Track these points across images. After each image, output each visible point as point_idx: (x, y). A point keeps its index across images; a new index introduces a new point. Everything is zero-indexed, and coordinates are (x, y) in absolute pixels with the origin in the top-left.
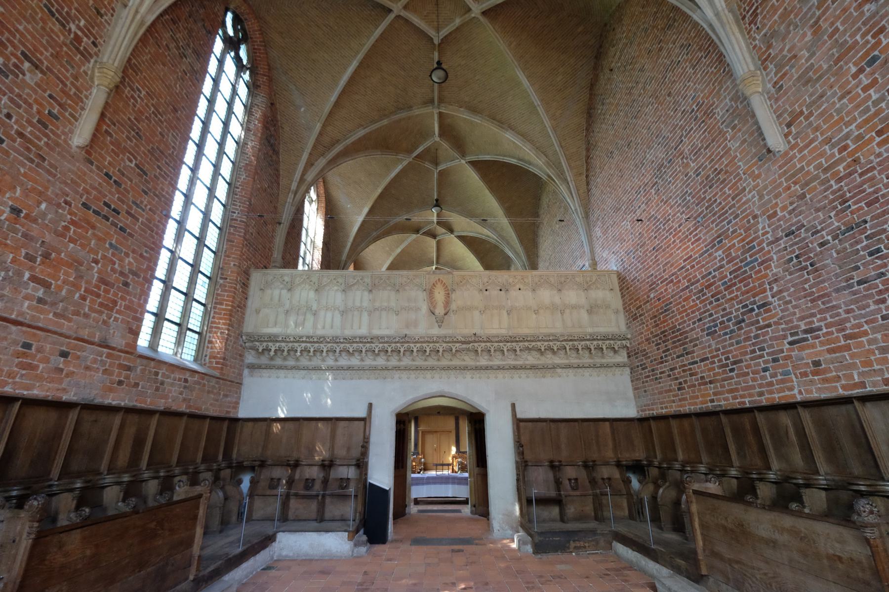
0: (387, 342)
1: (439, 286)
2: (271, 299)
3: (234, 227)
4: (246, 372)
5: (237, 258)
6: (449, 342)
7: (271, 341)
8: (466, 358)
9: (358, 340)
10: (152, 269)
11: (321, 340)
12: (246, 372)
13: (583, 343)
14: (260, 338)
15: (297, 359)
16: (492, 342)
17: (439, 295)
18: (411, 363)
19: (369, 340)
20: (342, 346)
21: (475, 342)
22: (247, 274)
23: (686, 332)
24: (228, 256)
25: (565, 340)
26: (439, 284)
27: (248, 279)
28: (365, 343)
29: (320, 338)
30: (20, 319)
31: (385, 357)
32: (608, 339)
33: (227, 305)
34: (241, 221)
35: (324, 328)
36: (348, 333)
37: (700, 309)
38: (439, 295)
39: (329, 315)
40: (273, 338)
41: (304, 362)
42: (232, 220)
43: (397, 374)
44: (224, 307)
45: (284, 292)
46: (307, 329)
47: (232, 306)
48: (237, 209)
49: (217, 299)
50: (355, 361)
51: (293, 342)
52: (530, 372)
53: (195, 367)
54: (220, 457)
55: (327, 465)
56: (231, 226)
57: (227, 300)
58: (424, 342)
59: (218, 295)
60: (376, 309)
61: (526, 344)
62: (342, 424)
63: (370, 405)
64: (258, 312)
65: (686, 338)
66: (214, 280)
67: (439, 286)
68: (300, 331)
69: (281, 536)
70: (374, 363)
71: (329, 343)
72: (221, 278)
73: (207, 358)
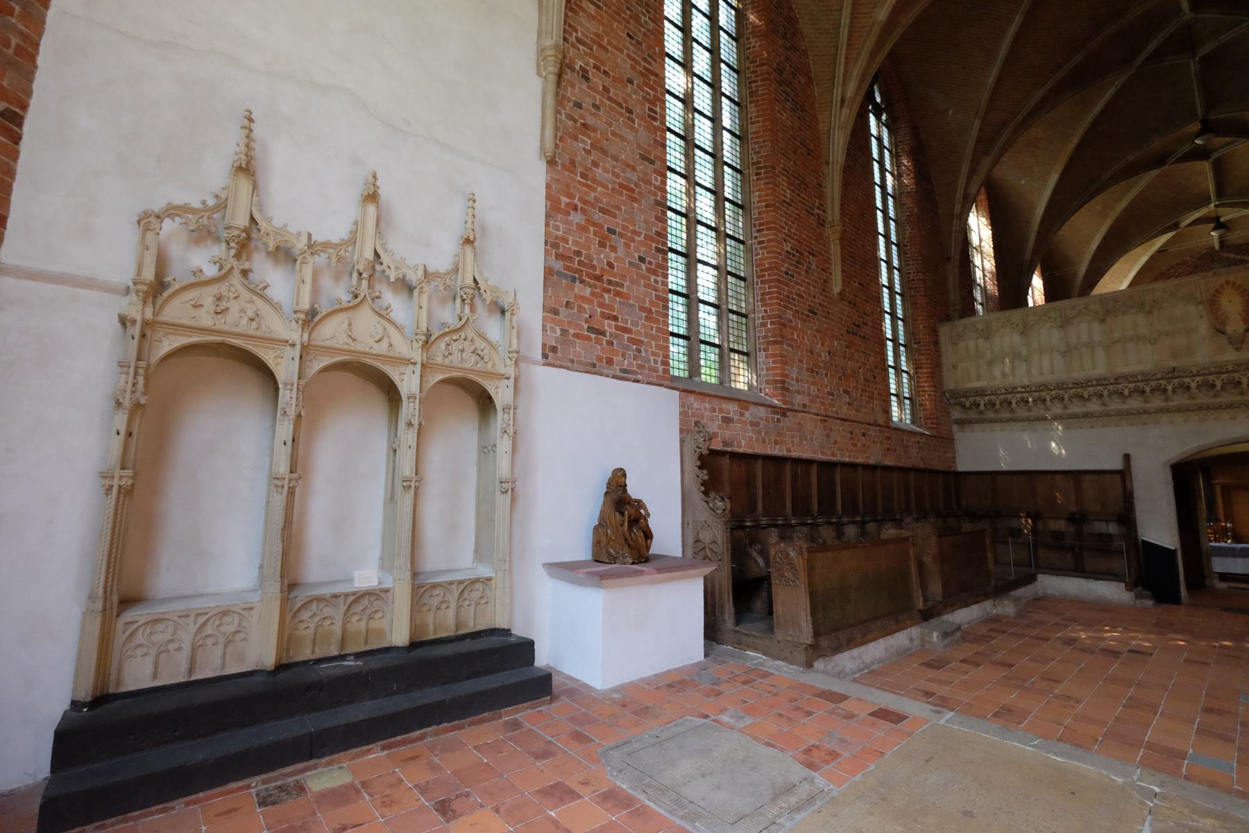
0: (1141, 381)
4: (955, 428)
7: (978, 395)
9: (1094, 382)
10: (885, 359)
11: (1042, 388)
12: (955, 428)
14: (966, 394)
15: (1012, 411)
19: (1112, 381)
22: (934, 332)
28: (1106, 385)
29: (1040, 386)
30: (856, 419)
31: (1141, 399)
33: (927, 368)
34: (918, 280)
35: (1041, 373)
36: (1078, 375)
40: (980, 392)
41: (1022, 413)
42: (909, 281)
43: (1165, 418)
45: (981, 341)
46: (1021, 377)
47: (931, 368)
49: (916, 364)
50: (1094, 406)
51: (1006, 394)
53: (914, 427)
54: (955, 507)
55: (1078, 519)
57: (926, 364)
59: (916, 360)
60: (1114, 342)
64: (955, 367)
68: (1011, 381)
69: (1040, 577)
70: (1125, 407)
71: (1052, 390)
72: (915, 343)
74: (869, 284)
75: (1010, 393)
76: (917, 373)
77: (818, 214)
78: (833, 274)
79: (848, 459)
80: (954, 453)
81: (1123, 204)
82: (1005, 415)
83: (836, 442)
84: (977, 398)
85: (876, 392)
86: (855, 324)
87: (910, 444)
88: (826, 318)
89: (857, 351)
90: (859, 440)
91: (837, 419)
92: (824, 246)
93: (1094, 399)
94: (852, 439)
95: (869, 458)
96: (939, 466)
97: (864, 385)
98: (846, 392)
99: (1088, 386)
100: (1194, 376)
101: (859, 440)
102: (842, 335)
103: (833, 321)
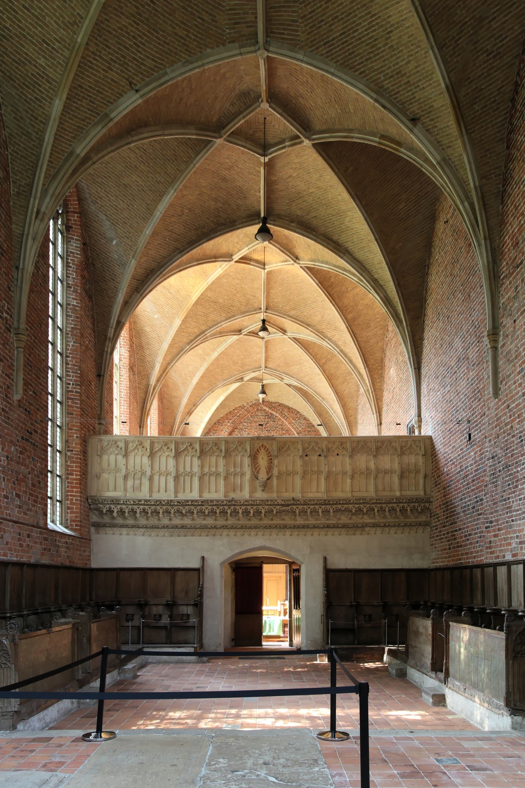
1: (262, 451)
2: (109, 465)
3: (73, 399)
5: (78, 430)
6: (270, 505)
8: (286, 518)
9: (190, 503)
12: (93, 529)
13: (390, 505)
14: (104, 501)
15: (136, 519)
16: (308, 504)
17: (263, 461)
18: (237, 522)
19: (200, 503)
20: (176, 508)
21: (293, 504)
23: (455, 507)
24: (71, 429)
25: (373, 503)
26: (262, 449)
27: (85, 446)
28: (197, 505)
29: (157, 501)
32: (412, 502)
36: (181, 497)
37: (462, 491)
38: (263, 461)
39: (163, 479)
40: (115, 501)
43: (225, 532)
44: (74, 477)
45: (120, 457)
48: (71, 380)
49: (68, 470)
50: (187, 521)
52: (343, 530)
56: (68, 398)
57: (76, 471)
58: (248, 505)
59: (68, 466)
61: (339, 506)
62: (179, 573)
63: (203, 558)
65: (455, 511)
66: (64, 452)
67: (262, 451)
71: (163, 505)
73: (69, 521)
74: (40, 393)
75: (136, 505)
76: (68, 478)
77: (6, 318)
78: (15, 381)
79: (15, 559)
80: (90, 552)
81: (216, 354)
82: (131, 522)
83: (7, 543)
84: (112, 506)
85: (40, 496)
86: (28, 431)
87: (60, 544)
88: (6, 423)
89: (29, 457)
90: (24, 541)
91: (10, 521)
92: (10, 352)
93: (189, 514)
94: (19, 540)
95: (30, 557)
96: (79, 564)
97: (32, 490)
98: (18, 495)
99: (187, 505)
100: (241, 505)
101: (24, 541)
102: (18, 441)
103: (12, 426)
